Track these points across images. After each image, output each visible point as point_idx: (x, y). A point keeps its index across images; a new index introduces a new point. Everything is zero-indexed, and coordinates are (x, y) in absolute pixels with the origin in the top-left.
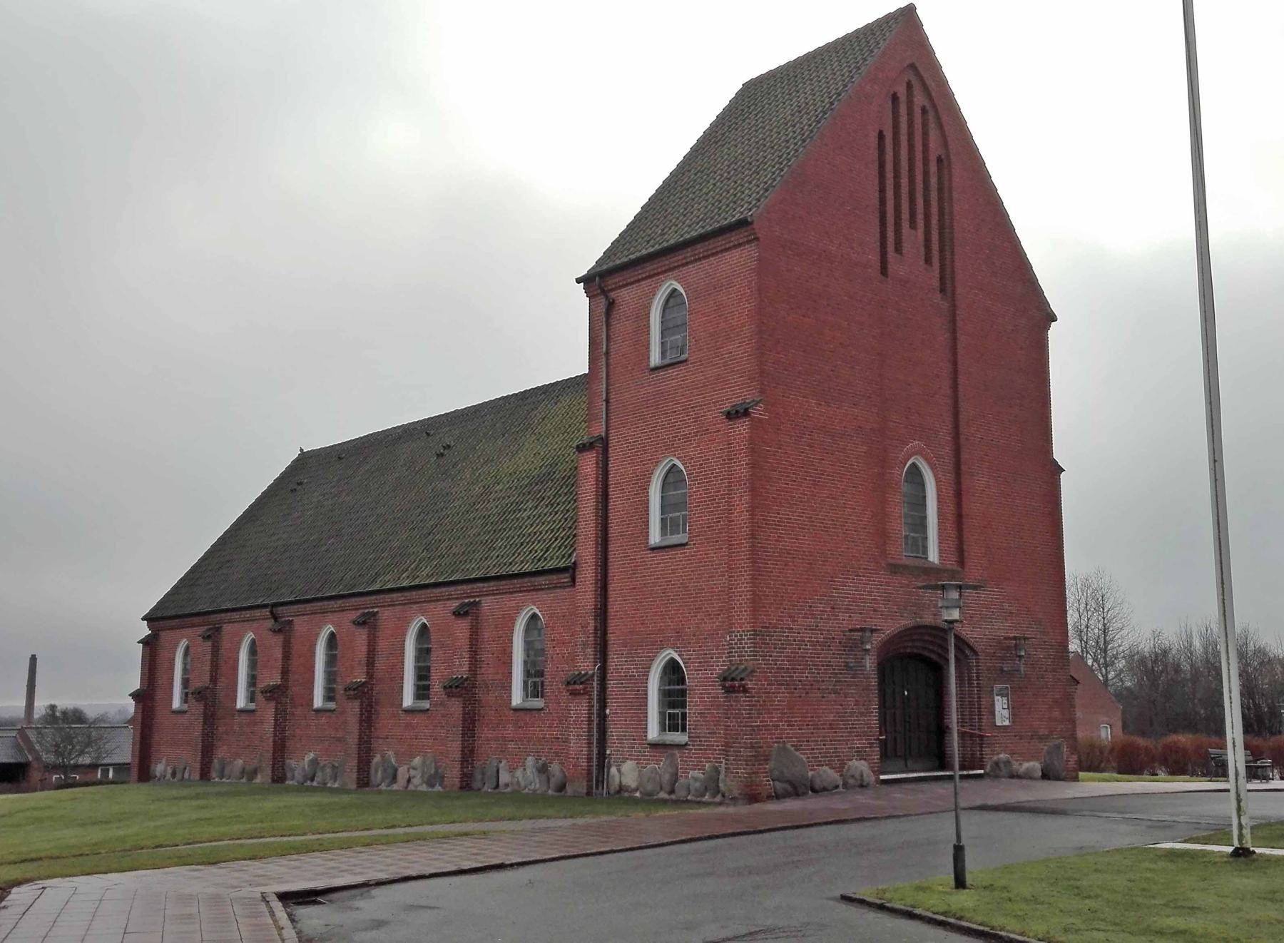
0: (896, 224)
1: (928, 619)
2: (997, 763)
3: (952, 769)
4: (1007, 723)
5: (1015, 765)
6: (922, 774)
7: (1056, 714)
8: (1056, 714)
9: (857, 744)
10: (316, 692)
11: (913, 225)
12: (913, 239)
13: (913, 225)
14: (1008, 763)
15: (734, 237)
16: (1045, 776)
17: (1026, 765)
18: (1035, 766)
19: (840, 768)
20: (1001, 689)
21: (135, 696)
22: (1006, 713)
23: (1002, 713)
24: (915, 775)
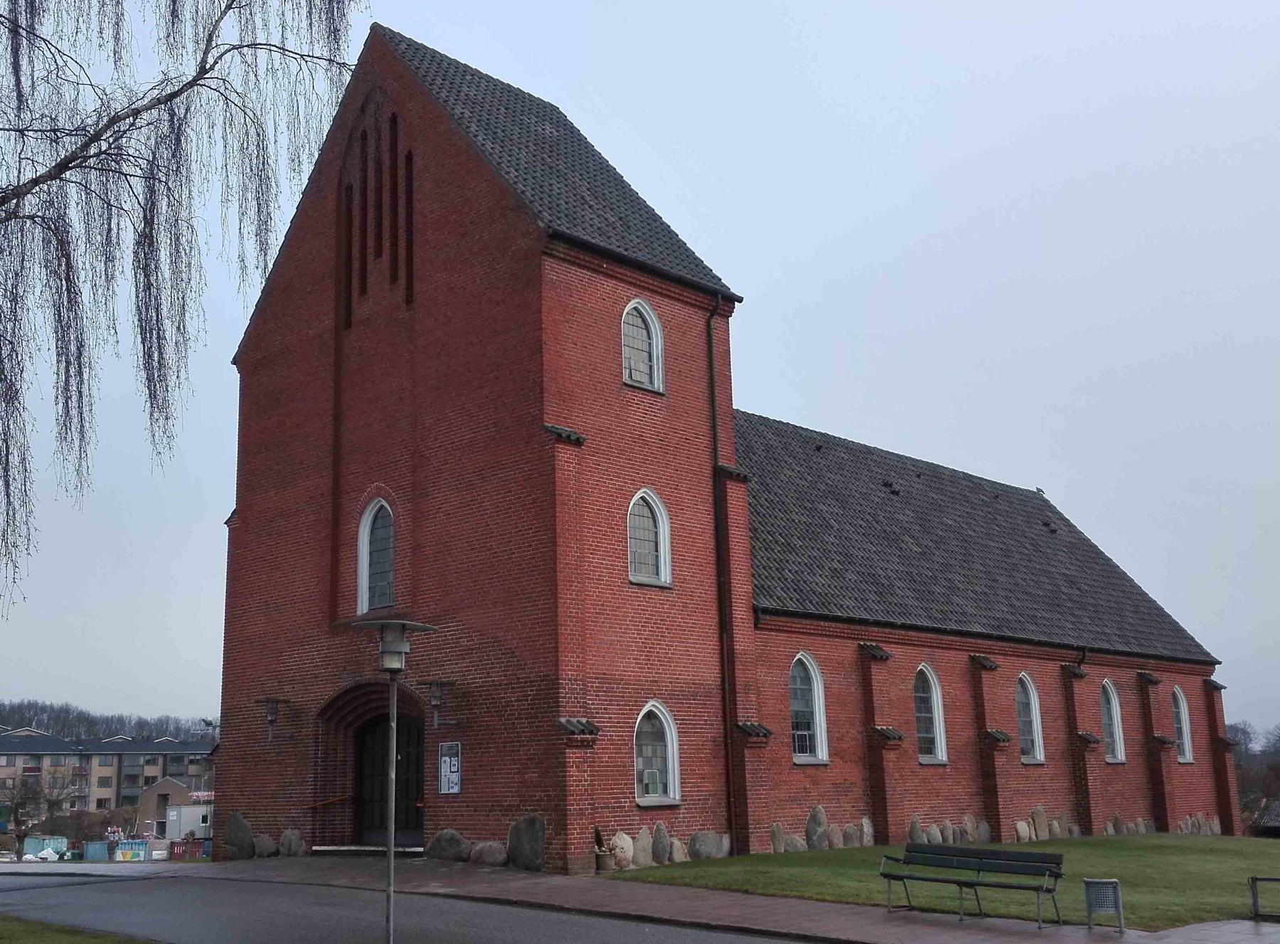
0: (396, 263)
1: (368, 675)
2: (438, 840)
3: (385, 844)
4: (456, 790)
5: (465, 844)
6: (353, 848)
7: (533, 776)
8: (533, 776)
9: (294, 813)
10: (823, 718)
11: (379, 253)
12: (378, 270)
13: (379, 253)
14: (452, 840)
15: (700, 297)
16: (513, 862)
17: (481, 845)
18: (495, 847)
19: (277, 837)
20: (451, 748)
21: (1218, 688)
22: (455, 778)
23: (449, 775)
24: (353, 848)
